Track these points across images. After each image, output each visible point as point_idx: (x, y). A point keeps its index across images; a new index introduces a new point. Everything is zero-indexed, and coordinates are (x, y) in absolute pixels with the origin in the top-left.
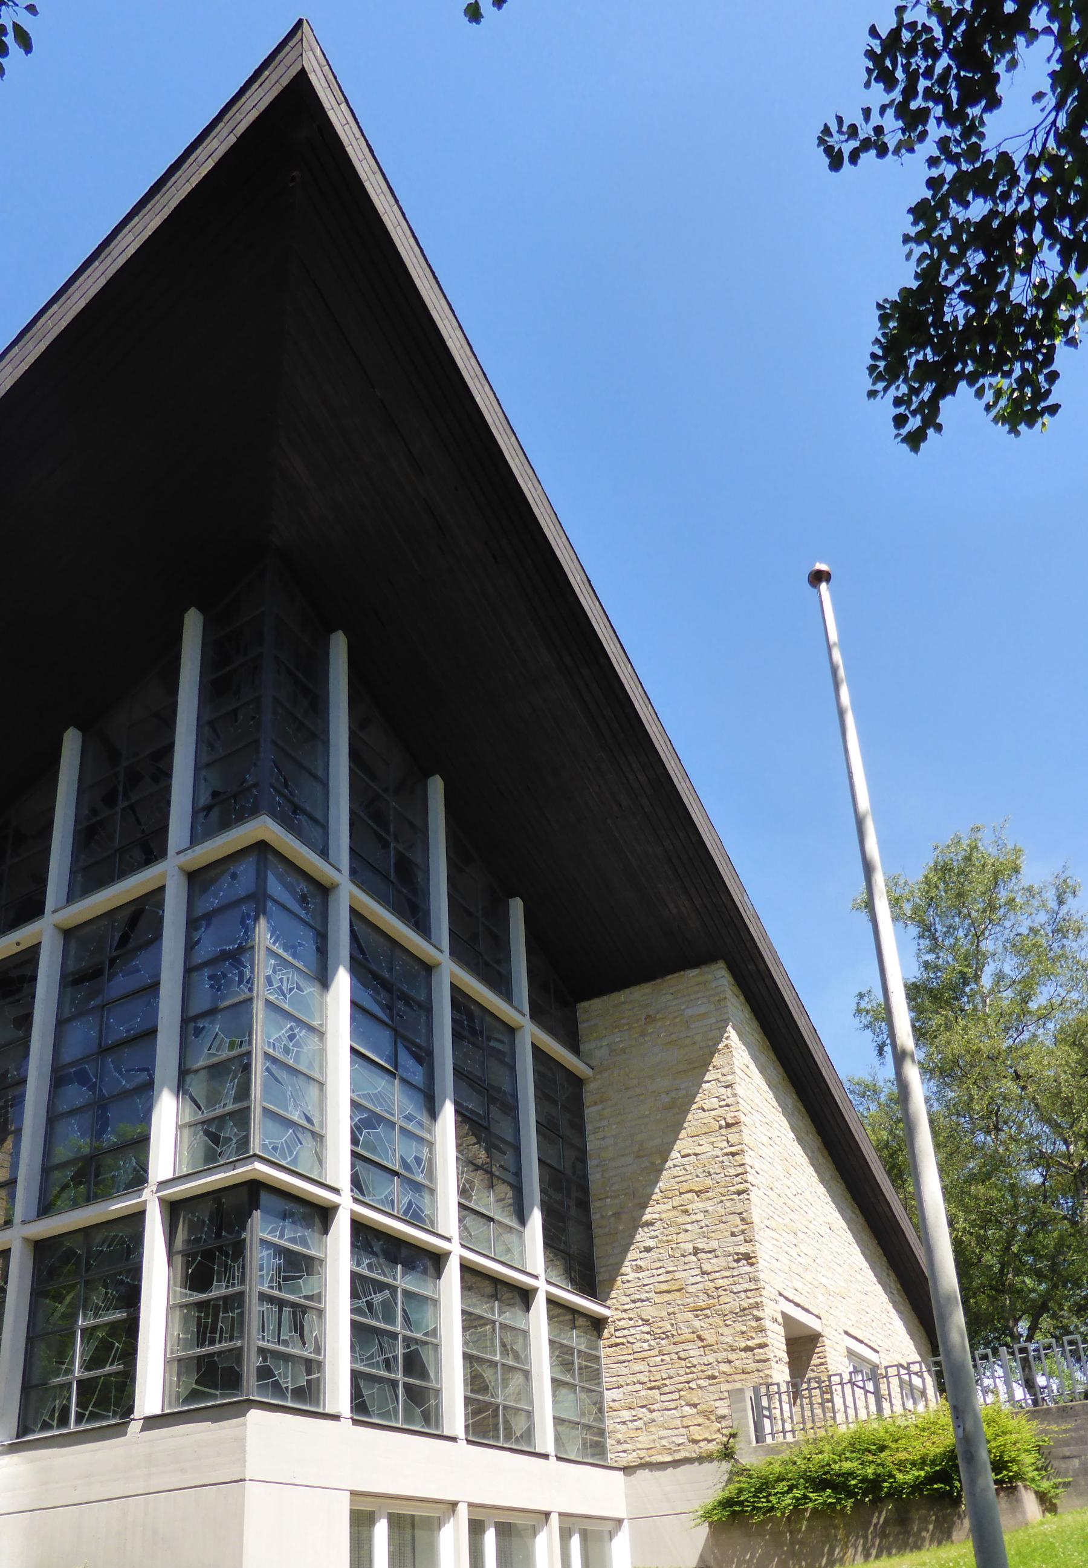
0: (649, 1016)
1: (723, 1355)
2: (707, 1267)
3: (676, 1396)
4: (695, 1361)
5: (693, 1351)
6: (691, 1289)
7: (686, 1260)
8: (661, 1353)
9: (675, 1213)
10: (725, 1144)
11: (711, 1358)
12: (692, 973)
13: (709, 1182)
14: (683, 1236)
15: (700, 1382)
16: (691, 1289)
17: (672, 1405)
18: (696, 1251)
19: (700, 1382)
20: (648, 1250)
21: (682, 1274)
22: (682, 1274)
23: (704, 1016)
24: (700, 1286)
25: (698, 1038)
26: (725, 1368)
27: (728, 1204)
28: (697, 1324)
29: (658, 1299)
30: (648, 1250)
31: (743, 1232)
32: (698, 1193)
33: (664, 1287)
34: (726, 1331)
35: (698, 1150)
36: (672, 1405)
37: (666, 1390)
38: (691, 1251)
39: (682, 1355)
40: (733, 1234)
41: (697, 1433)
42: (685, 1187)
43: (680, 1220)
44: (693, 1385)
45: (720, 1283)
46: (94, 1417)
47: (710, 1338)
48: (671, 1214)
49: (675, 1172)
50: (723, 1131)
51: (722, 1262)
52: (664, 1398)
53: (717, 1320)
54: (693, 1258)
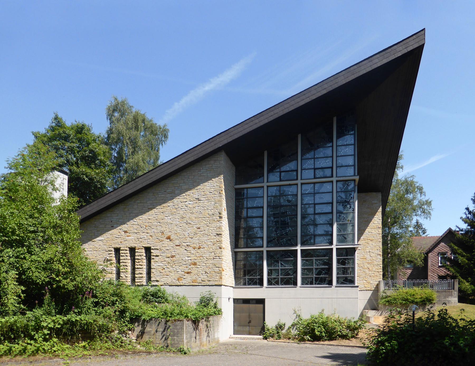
0: (364, 201)
1: (373, 272)
2: (371, 255)
3: (362, 279)
4: (367, 273)
5: (367, 271)
6: (368, 259)
7: (367, 253)
8: (360, 270)
9: (366, 243)
10: (378, 232)
11: (370, 273)
12: (375, 193)
13: (373, 239)
14: (367, 248)
15: (368, 277)
16: (368, 259)
17: (361, 280)
18: (369, 252)
19: (368, 277)
20: (360, 250)
21: (366, 256)
22: (366, 256)
23: (376, 203)
24: (370, 259)
25: (374, 208)
26: (373, 275)
27: (377, 244)
28: (368, 266)
29: (361, 260)
30: (360, 250)
31: (379, 250)
32: (371, 240)
33: (362, 258)
34: (374, 268)
35: (372, 232)
36: (361, 280)
37: (361, 277)
38: (368, 251)
39: (365, 271)
40: (377, 250)
41: (366, 286)
42: (368, 238)
43: (367, 245)
44: (366, 277)
45: (374, 259)
46: (318, 284)
47: (371, 269)
48: (365, 243)
49: (367, 235)
50: (378, 229)
51: (375, 255)
52: (360, 279)
53: (372, 266)
54: (369, 253)
